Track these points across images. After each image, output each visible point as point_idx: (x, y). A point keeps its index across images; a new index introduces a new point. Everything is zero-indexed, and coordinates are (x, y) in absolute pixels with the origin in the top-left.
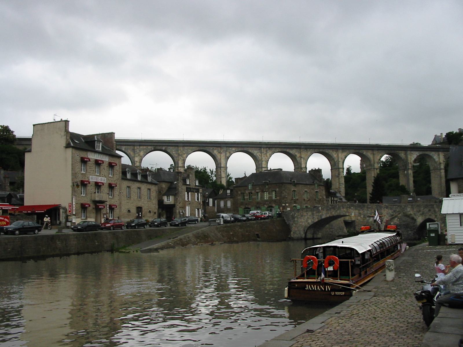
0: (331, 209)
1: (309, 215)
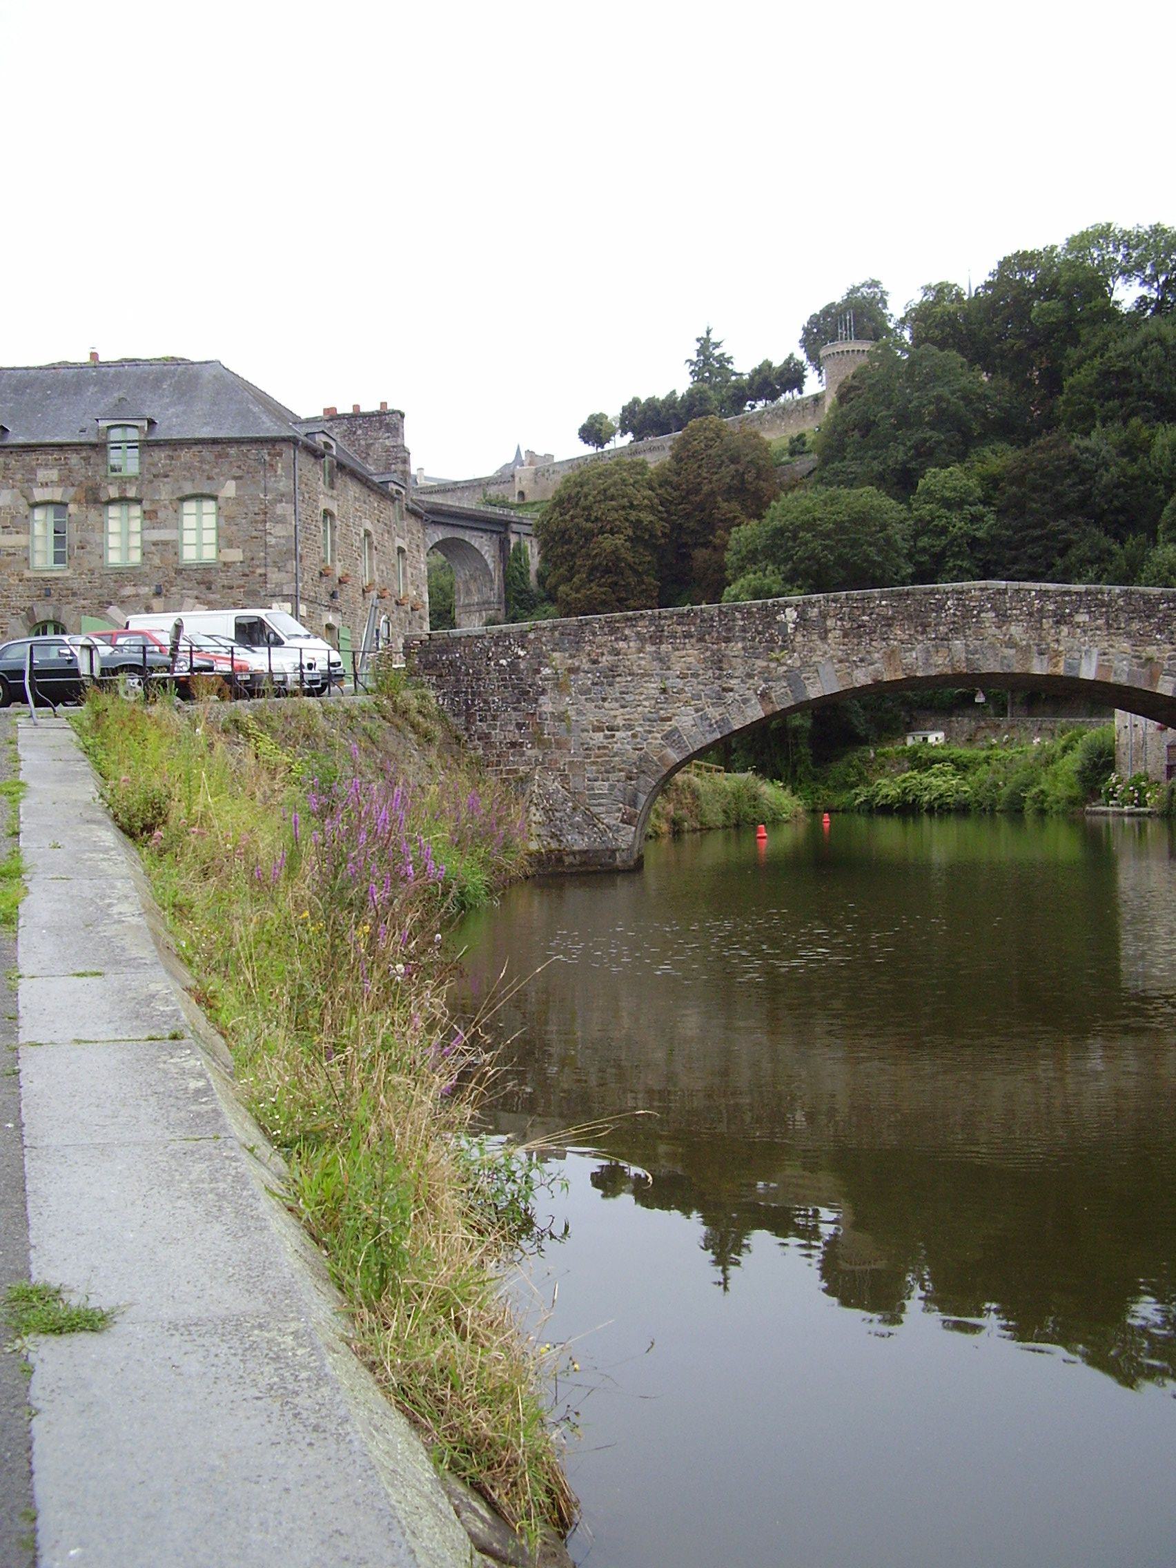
0: (889, 622)
1: (677, 668)
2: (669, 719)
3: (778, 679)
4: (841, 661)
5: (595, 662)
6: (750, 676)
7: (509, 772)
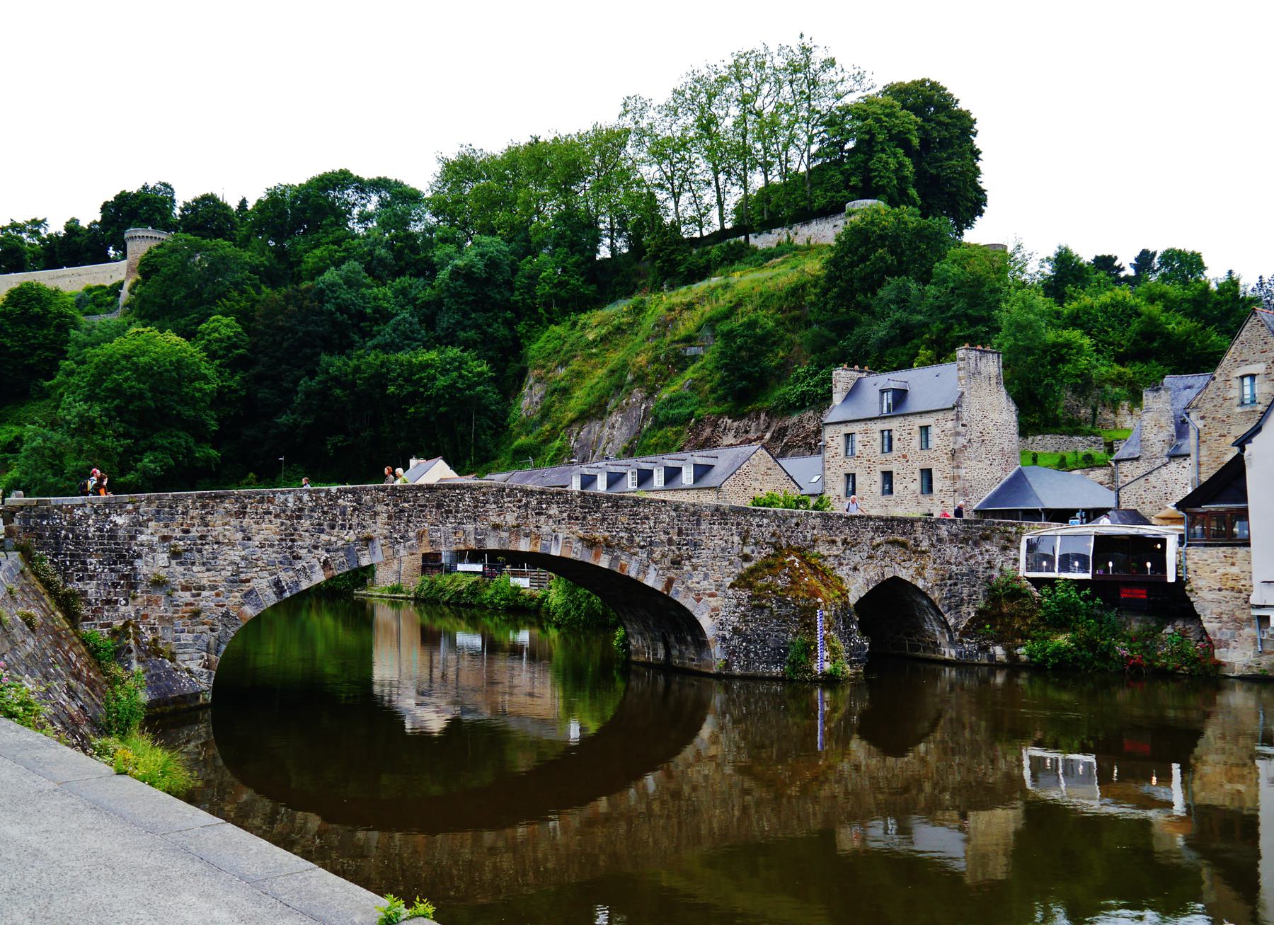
1: (257, 539)
2: (248, 581)
3: (338, 550)
4: (386, 538)
5: (187, 531)
6: (316, 547)
7: (102, 626)
